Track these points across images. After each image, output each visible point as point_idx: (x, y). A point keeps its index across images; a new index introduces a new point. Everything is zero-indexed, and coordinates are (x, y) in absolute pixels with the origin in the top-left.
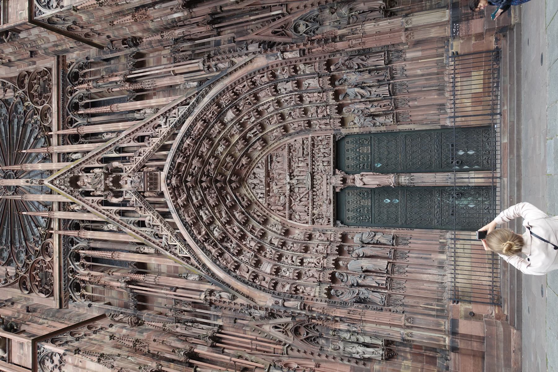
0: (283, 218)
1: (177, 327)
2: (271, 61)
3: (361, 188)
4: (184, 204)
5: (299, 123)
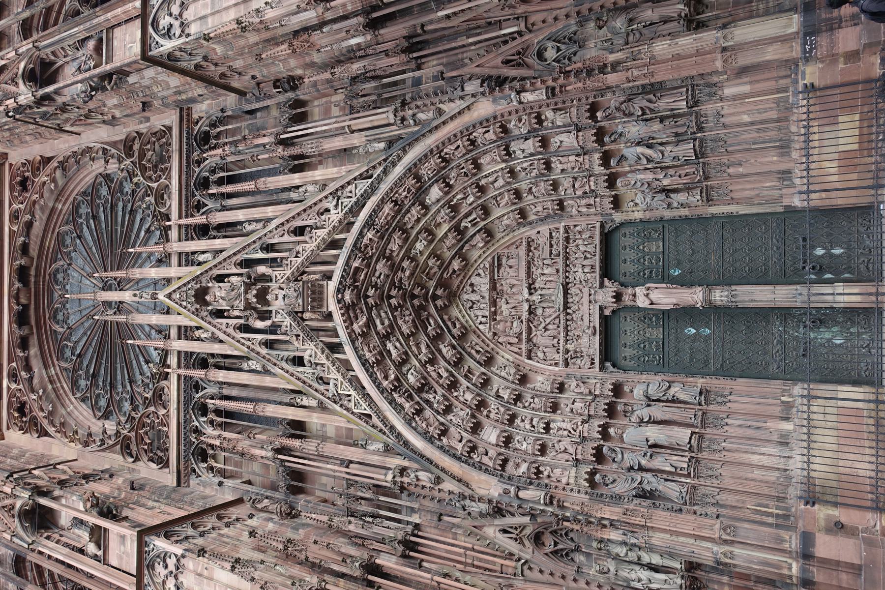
0: (517, 356)
1: (350, 522)
2: (500, 107)
3: (645, 309)
4: (363, 332)
5: (544, 204)
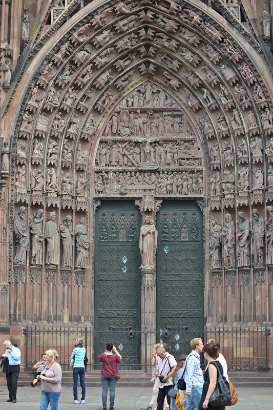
0: (102, 132)
4: (117, 11)
5: (218, 157)
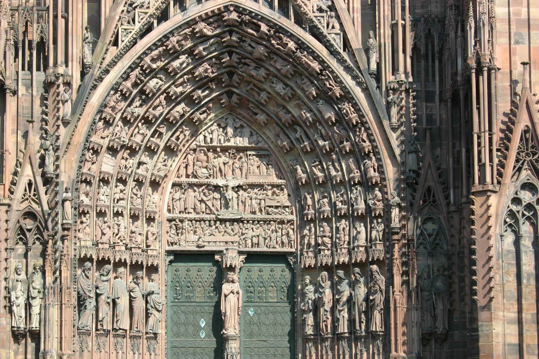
4: (197, 33)
